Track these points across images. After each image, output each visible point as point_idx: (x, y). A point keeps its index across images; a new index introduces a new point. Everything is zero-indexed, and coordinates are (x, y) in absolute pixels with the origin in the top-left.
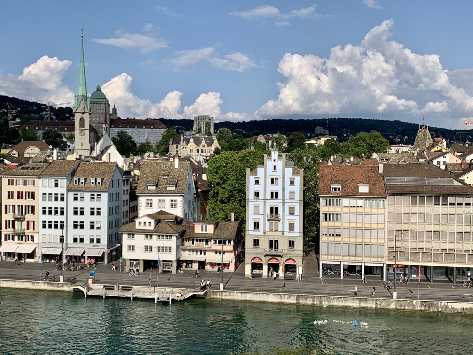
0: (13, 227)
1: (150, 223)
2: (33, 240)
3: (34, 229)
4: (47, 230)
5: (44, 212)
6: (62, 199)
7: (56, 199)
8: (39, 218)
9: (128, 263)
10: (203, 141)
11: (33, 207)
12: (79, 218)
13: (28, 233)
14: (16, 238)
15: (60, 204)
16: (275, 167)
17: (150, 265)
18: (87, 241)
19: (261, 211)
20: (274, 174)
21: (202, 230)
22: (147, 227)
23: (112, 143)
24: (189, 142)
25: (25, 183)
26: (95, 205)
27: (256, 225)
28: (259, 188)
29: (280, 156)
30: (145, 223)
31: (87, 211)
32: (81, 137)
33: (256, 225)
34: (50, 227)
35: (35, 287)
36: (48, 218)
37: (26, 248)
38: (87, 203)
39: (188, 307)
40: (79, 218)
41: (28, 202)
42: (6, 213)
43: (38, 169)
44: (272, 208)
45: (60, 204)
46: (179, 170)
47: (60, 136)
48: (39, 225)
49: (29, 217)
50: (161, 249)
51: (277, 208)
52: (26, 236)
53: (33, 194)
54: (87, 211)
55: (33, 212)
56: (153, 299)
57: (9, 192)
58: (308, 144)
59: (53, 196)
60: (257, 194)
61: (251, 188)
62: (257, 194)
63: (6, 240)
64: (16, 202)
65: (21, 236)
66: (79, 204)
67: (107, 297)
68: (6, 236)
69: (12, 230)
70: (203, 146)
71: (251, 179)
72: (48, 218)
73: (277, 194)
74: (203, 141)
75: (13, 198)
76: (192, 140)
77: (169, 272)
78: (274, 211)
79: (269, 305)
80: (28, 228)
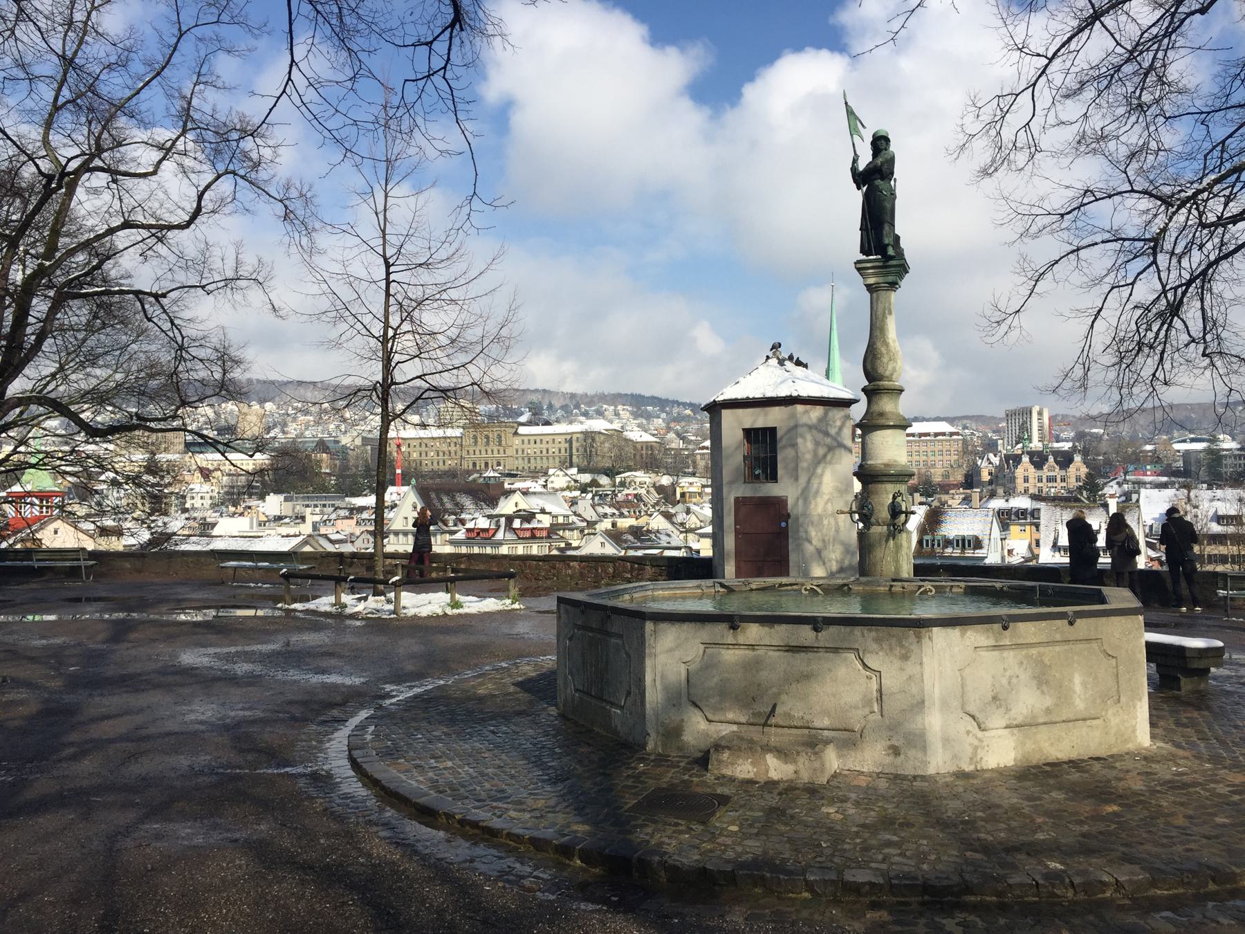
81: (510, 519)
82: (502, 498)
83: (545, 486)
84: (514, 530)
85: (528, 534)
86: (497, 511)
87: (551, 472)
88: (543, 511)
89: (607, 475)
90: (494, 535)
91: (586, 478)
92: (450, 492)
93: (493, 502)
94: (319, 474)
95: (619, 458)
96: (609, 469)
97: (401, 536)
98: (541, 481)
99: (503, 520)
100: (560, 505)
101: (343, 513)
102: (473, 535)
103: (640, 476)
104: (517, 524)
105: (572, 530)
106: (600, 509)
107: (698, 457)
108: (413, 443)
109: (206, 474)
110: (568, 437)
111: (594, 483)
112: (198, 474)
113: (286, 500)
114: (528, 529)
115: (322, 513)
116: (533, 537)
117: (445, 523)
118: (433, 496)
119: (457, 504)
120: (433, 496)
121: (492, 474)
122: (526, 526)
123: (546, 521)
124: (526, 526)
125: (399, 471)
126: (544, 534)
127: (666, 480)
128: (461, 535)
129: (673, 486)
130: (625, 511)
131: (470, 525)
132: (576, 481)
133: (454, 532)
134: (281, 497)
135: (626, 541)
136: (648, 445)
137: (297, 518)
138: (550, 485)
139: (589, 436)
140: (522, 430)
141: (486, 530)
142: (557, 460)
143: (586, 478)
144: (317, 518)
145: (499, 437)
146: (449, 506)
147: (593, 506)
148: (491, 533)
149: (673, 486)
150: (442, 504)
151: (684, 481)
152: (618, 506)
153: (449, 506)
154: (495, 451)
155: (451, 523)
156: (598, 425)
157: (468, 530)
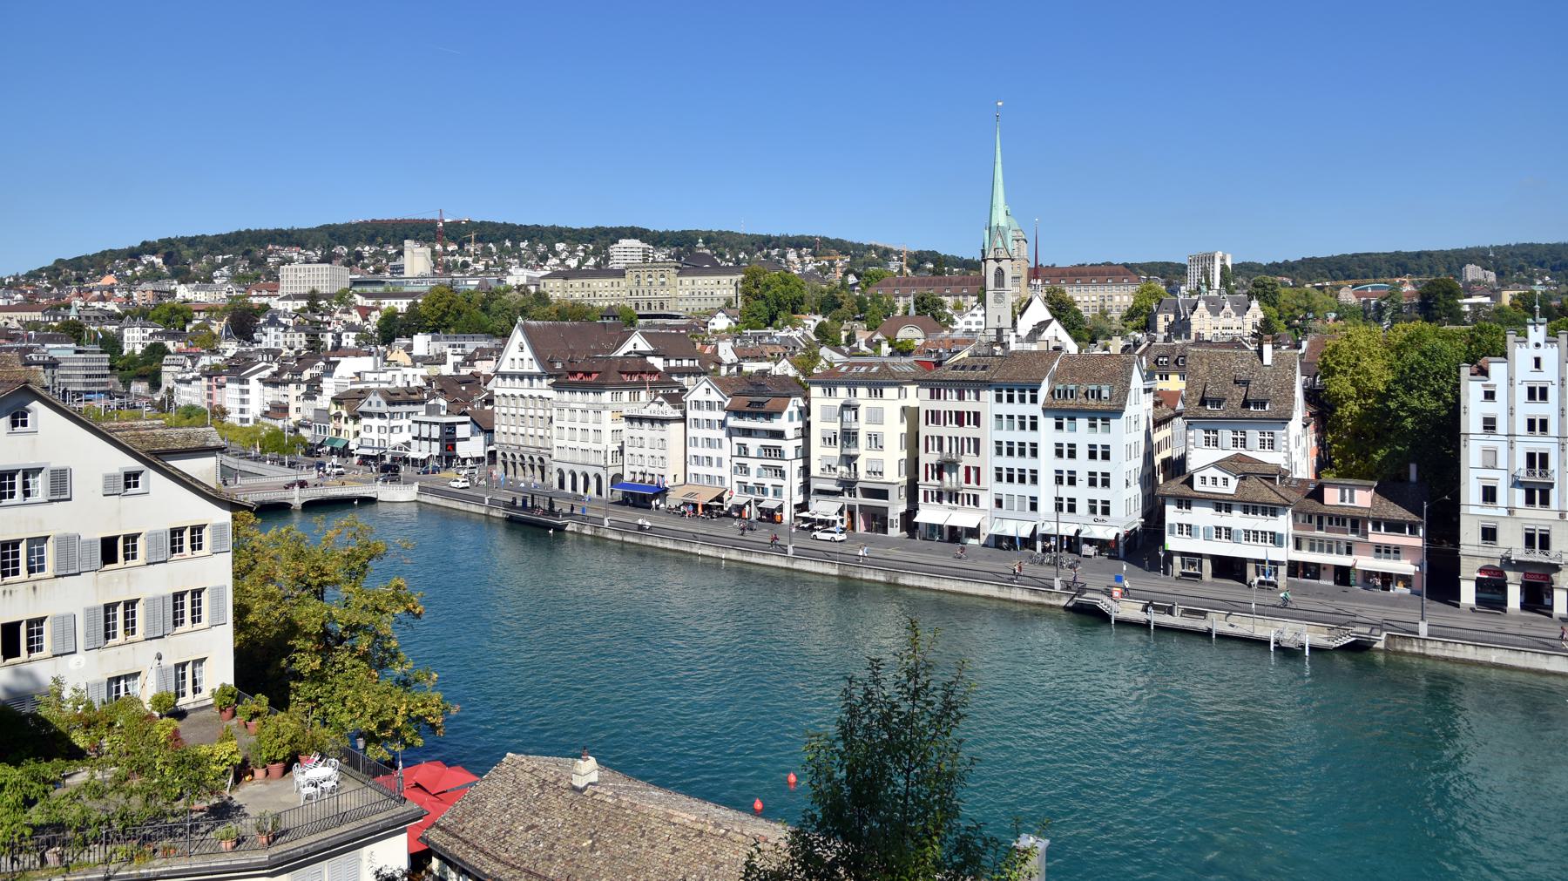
1: (1225, 480)
2: (976, 503)
3: (978, 482)
6: (1034, 427)
7: (1023, 426)
8: (989, 461)
9: (1177, 560)
10: (1228, 306)
12: (1066, 464)
13: (970, 489)
14: (945, 496)
15: (1027, 436)
16: (1538, 362)
17: (1229, 568)
18: (1082, 507)
19: (1502, 462)
20: (1538, 379)
21: (1343, 500)
22: (1220, 489)
23: (1049, 317)
24: (1195, 308)
25: (961, 397)
26: (1099, 438)
27: (1489, 494)
28: (1497, 409)
29: (1552, 335)
30: (1214, 479)
31: (1082, 452)
33: (1489, 494)
34: (1010, 479)
35: (1005, 594)
36: (1005, 462)
37: (962, 518)
38: (1081, 434)
39: (1342, 662)
40: (1066, 464)
41: (969, 431)
43: (984, 368)
44: (1531, 457)
45: (1027, 436)
46: (1273, 368)
47: (942, 304)
48: (988, 476)
50: (1252, 535)
51: (1544, 458)
53: (977, 415)
54: (1082, 452)
55: (977, 451)
56: (1266, 643)
58: (1471, 305)
59: (1016, 420)
60: (1489, 425)
61: (1474, 409)
62: (1489, 425)
63: (926, 500)
65: (953, 496)
66: (1065, 437)
67: (1159, 628)
68: (926, 493)
69: (937, 482)
70: (1228, 315)
71: (1472, 391)
72: (1005, 462)
73: (1544, 424)
74: (1228, 306)
76: (1202, 305)
77: (1270, 584)
78: (1537, 461)
79: (1551, 679)
80: (968, 481)
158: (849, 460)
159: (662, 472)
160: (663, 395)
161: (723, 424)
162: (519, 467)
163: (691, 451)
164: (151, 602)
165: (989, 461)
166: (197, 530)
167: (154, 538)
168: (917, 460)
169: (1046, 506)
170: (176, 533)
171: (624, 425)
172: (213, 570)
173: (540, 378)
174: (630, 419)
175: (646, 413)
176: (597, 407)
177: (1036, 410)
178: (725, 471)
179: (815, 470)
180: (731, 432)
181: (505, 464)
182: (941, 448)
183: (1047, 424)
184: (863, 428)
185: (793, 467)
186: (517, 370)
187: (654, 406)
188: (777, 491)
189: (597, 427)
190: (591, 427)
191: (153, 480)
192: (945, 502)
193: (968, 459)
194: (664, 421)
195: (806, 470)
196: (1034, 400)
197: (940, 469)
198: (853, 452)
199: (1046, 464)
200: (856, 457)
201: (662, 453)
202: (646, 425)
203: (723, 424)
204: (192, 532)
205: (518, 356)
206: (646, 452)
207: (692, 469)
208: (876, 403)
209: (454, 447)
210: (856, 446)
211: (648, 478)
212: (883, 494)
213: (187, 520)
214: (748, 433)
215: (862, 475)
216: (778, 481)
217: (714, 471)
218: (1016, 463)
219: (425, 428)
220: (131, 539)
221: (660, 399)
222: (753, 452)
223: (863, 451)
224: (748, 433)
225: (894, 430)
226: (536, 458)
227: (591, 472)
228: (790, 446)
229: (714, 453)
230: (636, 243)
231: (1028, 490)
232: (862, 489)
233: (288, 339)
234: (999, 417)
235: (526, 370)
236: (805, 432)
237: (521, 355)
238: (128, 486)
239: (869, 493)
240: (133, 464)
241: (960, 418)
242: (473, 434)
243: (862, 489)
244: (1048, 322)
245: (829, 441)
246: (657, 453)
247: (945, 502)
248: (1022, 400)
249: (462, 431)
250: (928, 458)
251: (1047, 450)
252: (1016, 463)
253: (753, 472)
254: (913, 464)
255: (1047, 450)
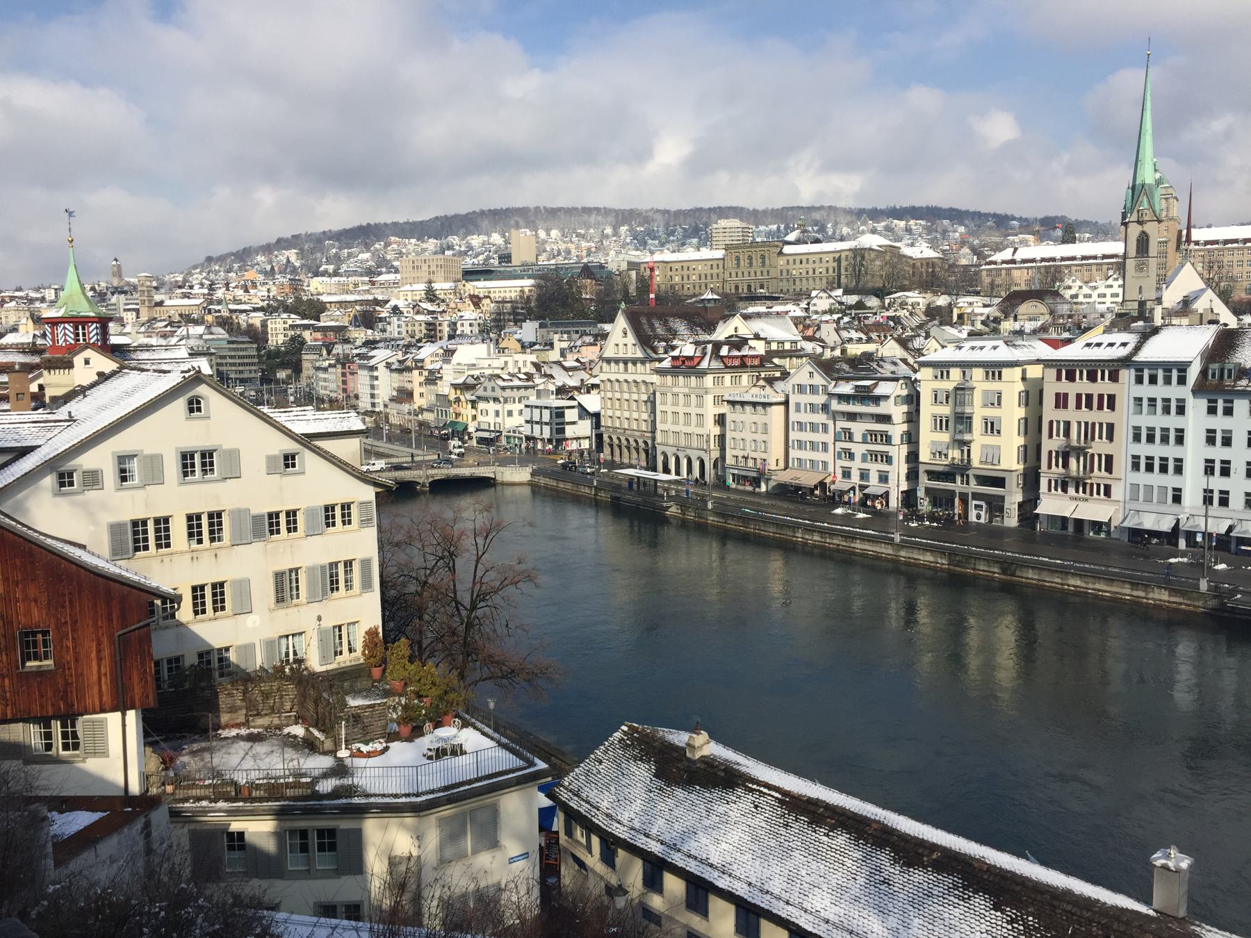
0: (1066, 465)
4: (1142, 478)
5: (1137, 438)
6: (1181, 410)
7: (1167, 410)
11: (1111, 427)
12: (1218, 453)
15: (1172, 422)
32: (1138, 274)
36: (1144, 449)
37: (1093, 510)
40: (1218, 453)
42: (1051, 436)
45: (1172, 422)
48: (1122, 464)
49: (1099, 447)
52: (1092, 485)
55: (1110, 438)
57: (1058, 395)
59: (1159, 404)
64: (1071, 414)
65: (1079, 483)
69: (1061, 470)
72: (1144, 449)
75: (1065, 406)
81: (717, 346)
82: (721, 323)
83: (807, 310)
84: (722, 357)
85: (737, 363)
86: (714, 337)
87: (814, 293)
88: (757, 337)
89: (877, 296)
90: (698, 364)
91: (852, 299)
92: (663, 318)
93: (710, 327)
94: (580, 300)
95: (890, 277)
96: (879, 289)
97: (639, 365)
98: (803, 305)
99: (710, 347)
100: (788, 330)
101: (588, 339)
102: (679, 363)
103: (914, 297)
104: (724, 351)
105: (801, 357)
106: (845, 334)
107: (984, 273)
108: (675, 266)
109: (476, 301)
110: (837, 255)
111: (860, 305)
112: (468, 301)
113: (541, 326)
114: (737, 357)
115: (570, 340)
116: (743, 366)
117: (655, 350)
118: (644, 321)
119: (669, 330)
120: (644, 321)
121: (710, 297)
122: (736, 353)
123: (760, 348)
124: (736, 353)
125: (652, 296)
126: (756, 362)
127: (942, 301)
128: (666, 364)
129: (950, 307)
130: (874, 335)
131: (676, 353)
132: (841, 303)
133: (661, 360)
134: (536, 324)
135: (838, 371)
136: (928, 262)
137: (546, 344)
138: (812, 308)
139: (859, 253)
140: (787, 249)
141: (691, 358)
142: (824, 280)
143: (852, 299)
144: (565, 345)
145: (763, 257)
146: (660, 331)
147: (837, 331)
148: (696, 361)
149: (950, 307)
150: (653, 329)
151: (963, 301)
152: (866, 330)
153: (660, 331)
154: (759, 273)
155: (661, 350)
156: (872, 241)
157: (674, 358)
158: (963, 444)
159: (764, 456)
160: (765, 379)
161: (825, 408)
162: (625, 451)
163: (793, 435)
164: (311, 570)
165: (1123, 449)
166: (346, 507)
167: (310, 512)
168: (1039, 447)
169: (1193, 498)
170: (329, 509)
171: (725, 409)
172: (360, 542)
173: (643, 362)
174: (733, 403)
175: (747, 398)
176: (700, 392)
177: (1185, 392)
178: (829, 457)
179: (925, 456)
180: (835, 416)
181: (611, 446)
182: (1067, 434)
183: (1197, 407)
184: (979, 412)
185: (899, 452)
186: (620, 355)
187: (756, 390)
188: (884, 478)
189: (700, 411)
190: (693, 410)
191: (308, 460)
192: (1071, 491)
193: (1099, 447)
194: (765, 405)
195: (913, 457)
196: (1182, 381)
197: (1065, 455)
198: (967, 437)
199: (1194, 452)
200: (970, 442)
201: (764, 437)
202: (748, 408)
203: (825, 408)
204: (343, 508)
205: (621, 341)
206: (749, 437)
207: (793, 454)
208: (994, 386)
209: (562, 431)
210: (970, 431)
211: (751, 463)
212: (999, 482)
213: (337, 498)
214: (852, 417)
215: (975, 462)
216: (884, 467)
217: (819, 456)
218: (1157, 450)
219: (536, 412)
220: (292, 514)
221: (762, 383)
222: (858, 437)
223: (979, 439)
224: (852, 417)
225: (1012, 413)
226: (641, 442)
227: (694, 455)
228: (897, 430)
229: (819, 437)
230: (735, 223)
231: (1170, 480)
232: (977, 477)
233: (410, 329)
234: (1139, 400)
235: (630, 355)
236: (913, 418)
237: (625, 341)
238: (287, 466)
239: (984, 480)
240: (291, 446)
241: (1087, 401)
242: (581, 418)
243: (977, 477)
244: (1202, 291)
245: (941, 423)
246: (760, 437)
247: (1071, 491)
248: (1168, 381)
249: (571, 415)
250: (1050, 445)
251: (1195, 437)
252: (1157, 450)
253: (858, 457)
254: (1031, 453)
255: (1195, 437)
